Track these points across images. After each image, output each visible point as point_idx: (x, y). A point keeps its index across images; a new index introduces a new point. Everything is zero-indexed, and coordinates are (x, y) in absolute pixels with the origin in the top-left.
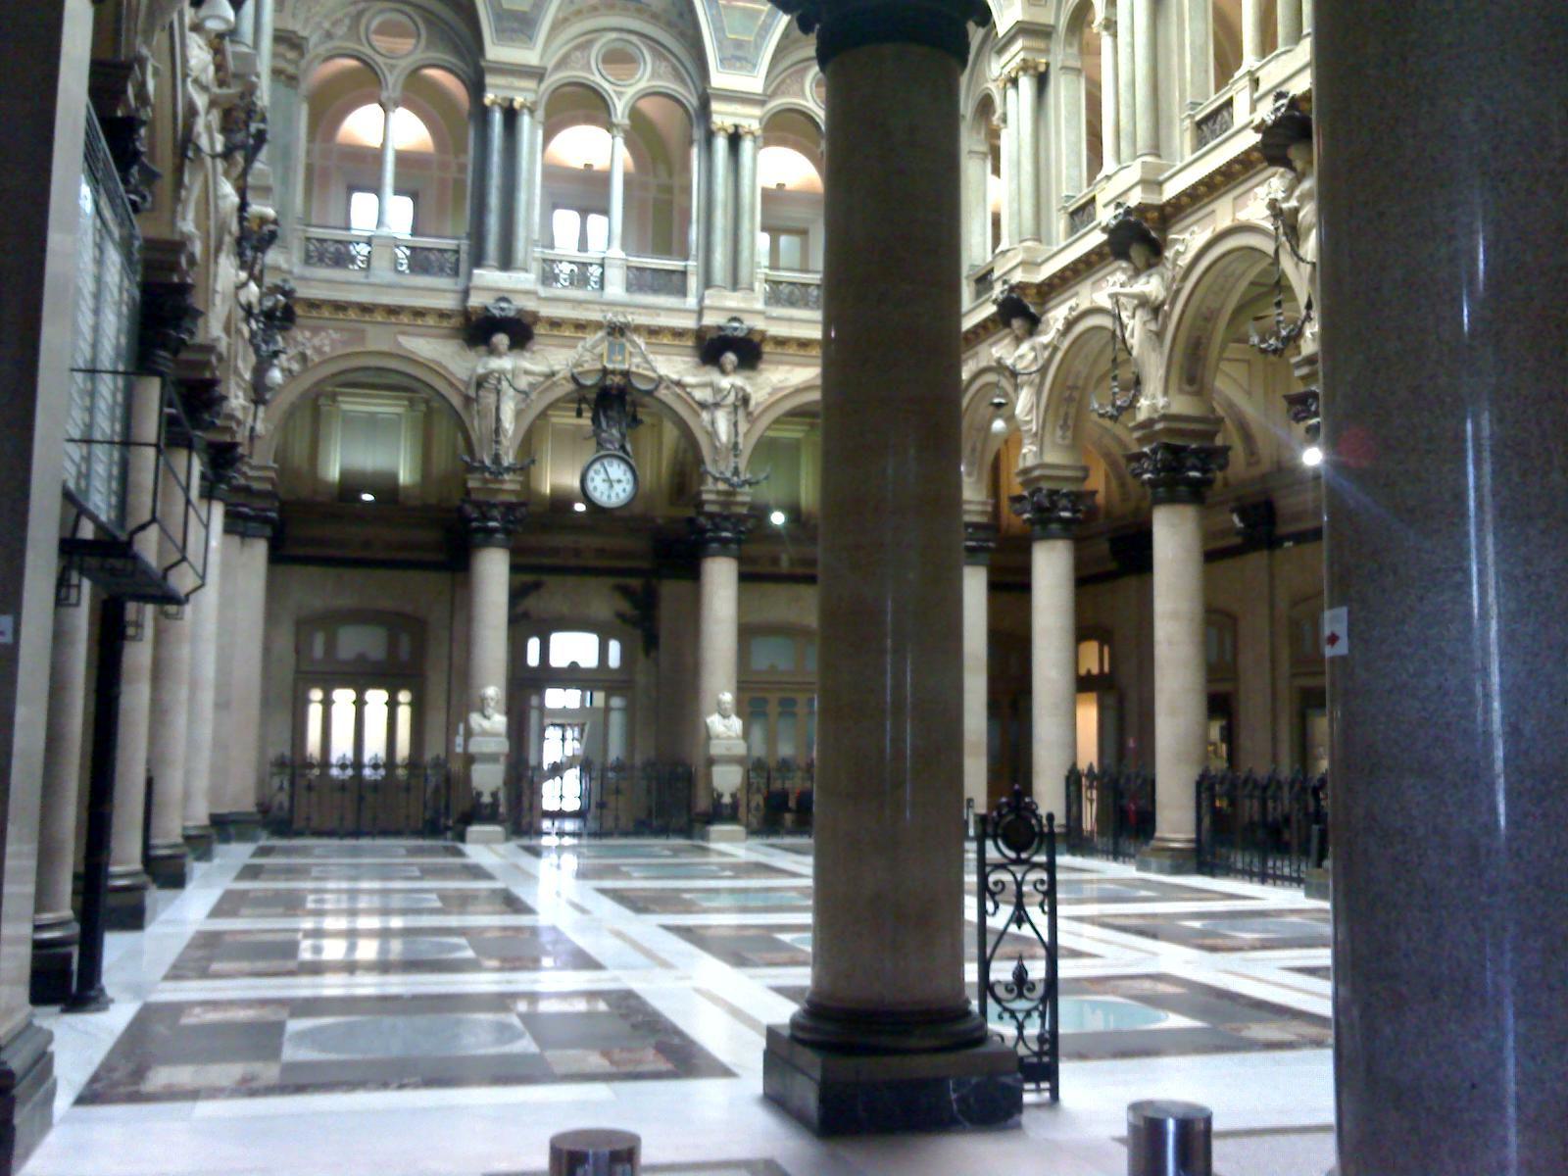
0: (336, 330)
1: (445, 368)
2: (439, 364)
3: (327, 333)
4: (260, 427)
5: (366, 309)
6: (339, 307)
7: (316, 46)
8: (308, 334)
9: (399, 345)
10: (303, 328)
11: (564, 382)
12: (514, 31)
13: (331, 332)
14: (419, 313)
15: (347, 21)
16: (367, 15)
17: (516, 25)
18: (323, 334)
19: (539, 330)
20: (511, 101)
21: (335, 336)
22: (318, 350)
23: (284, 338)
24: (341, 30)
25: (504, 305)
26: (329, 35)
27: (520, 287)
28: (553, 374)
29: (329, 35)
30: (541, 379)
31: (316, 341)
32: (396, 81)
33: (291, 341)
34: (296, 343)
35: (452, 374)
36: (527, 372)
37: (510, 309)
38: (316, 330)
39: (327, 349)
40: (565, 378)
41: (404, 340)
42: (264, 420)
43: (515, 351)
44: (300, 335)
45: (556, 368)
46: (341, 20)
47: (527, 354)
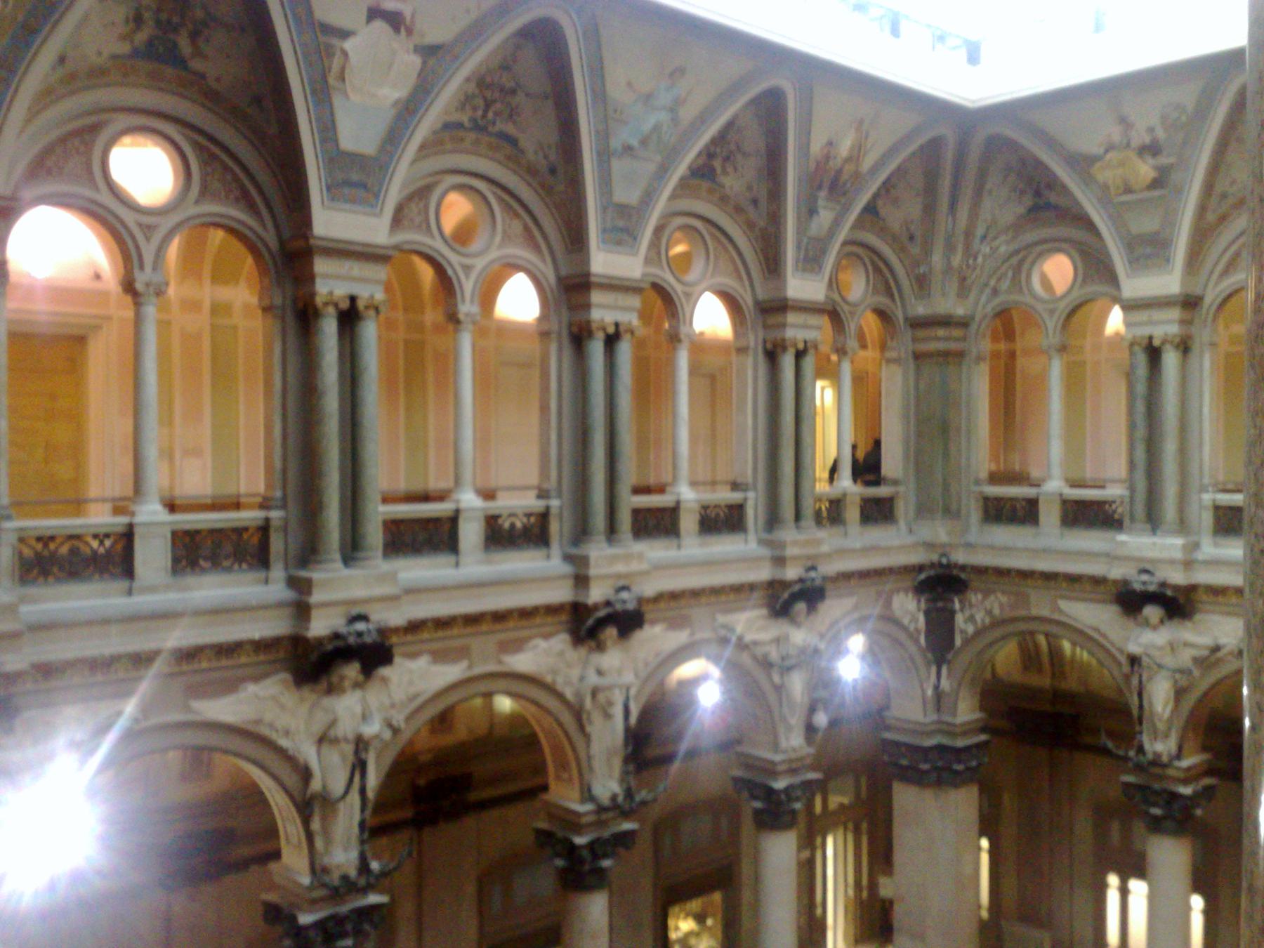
0: (1003, 592)
1: (1104, 636)
2: (1097, 630)
3: (996, 597)
4: (945, 684)
5: (1026, 575)
6: (1002, 573)
7: (984, 307)
8: (980, 596)
9: (1060, 611)
10: (976, 591)
11: (1230, 657)
12: (1148, 257)
13: (999, 595)
14: (1073, 579)
15: (1010, 274)
16: (1029, 260)
17: (1149, 250)
18: (992, 598)
19: (1202, 596)
20: (1151, 338)
21: (1004, 599)
22: (989, 613)
23: (961, 601)
24: (1005, 285)
25: (1145, 577)
26: (995, 292)
27: (1165, 555)
28: (1216, 649)
29: (995, 292)
30: (1206, 653)
31: (988, 604)
32: (1056, 326)
33: (967, 604)
34: (971, 606)
35: (1112, 644)
36: (1186, 644)
37: (1151, 583)
38: (987, 594)
39: (997, 611)
40: (1231, 653)
41: (1064, 605)
42: (949, 675)
43: (1176, 621)
44: (975, 598)
45: (1223, 640)
46: (1007, 271)
47: (1188, 624)
